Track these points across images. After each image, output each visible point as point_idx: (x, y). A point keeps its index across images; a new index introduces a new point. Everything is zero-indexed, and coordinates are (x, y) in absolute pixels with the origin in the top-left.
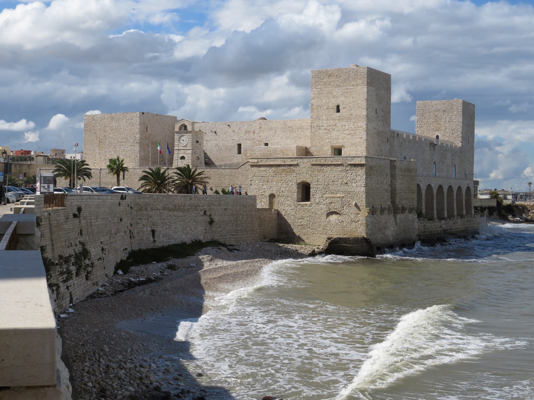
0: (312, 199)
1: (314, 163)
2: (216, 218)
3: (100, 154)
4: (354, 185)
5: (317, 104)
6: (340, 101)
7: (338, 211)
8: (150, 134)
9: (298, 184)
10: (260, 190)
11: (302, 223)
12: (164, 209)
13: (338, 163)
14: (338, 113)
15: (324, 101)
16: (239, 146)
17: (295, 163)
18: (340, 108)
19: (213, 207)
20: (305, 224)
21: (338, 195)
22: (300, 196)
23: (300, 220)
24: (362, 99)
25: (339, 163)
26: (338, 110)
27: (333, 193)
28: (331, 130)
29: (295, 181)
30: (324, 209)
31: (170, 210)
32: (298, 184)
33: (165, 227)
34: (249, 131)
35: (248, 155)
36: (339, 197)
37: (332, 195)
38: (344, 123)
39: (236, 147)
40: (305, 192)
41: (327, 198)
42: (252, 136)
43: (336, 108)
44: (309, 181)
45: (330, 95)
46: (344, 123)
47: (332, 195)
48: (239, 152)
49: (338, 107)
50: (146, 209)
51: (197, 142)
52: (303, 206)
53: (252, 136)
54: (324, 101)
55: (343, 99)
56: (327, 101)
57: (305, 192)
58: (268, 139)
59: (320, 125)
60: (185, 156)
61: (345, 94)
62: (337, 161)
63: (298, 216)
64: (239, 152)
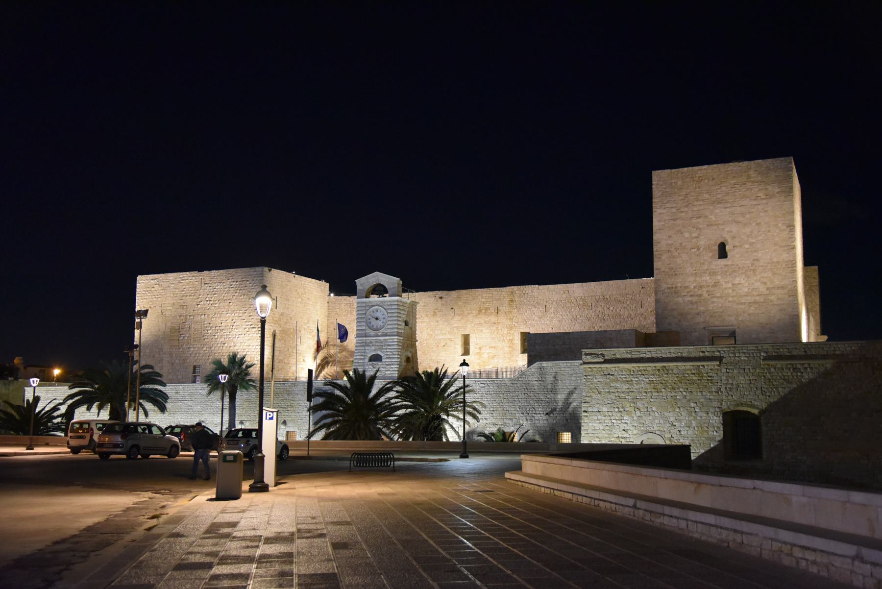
3: (171, 354)
5: (670, 242)
6: (728, 233)
8: (282, 314)
14: (723, 261)
15: (687, 235)
18: (727, 248)
24: (785, 227)
34: (486, 309)
35: (485, 356)
43: (717, 248)
45: (700, 220)
46: (737, 281)
54: (687, 235)
55: (734, 228)
56: (694, 235)
59: (679, 285)
60: (379, 353)
61: (741, 219)
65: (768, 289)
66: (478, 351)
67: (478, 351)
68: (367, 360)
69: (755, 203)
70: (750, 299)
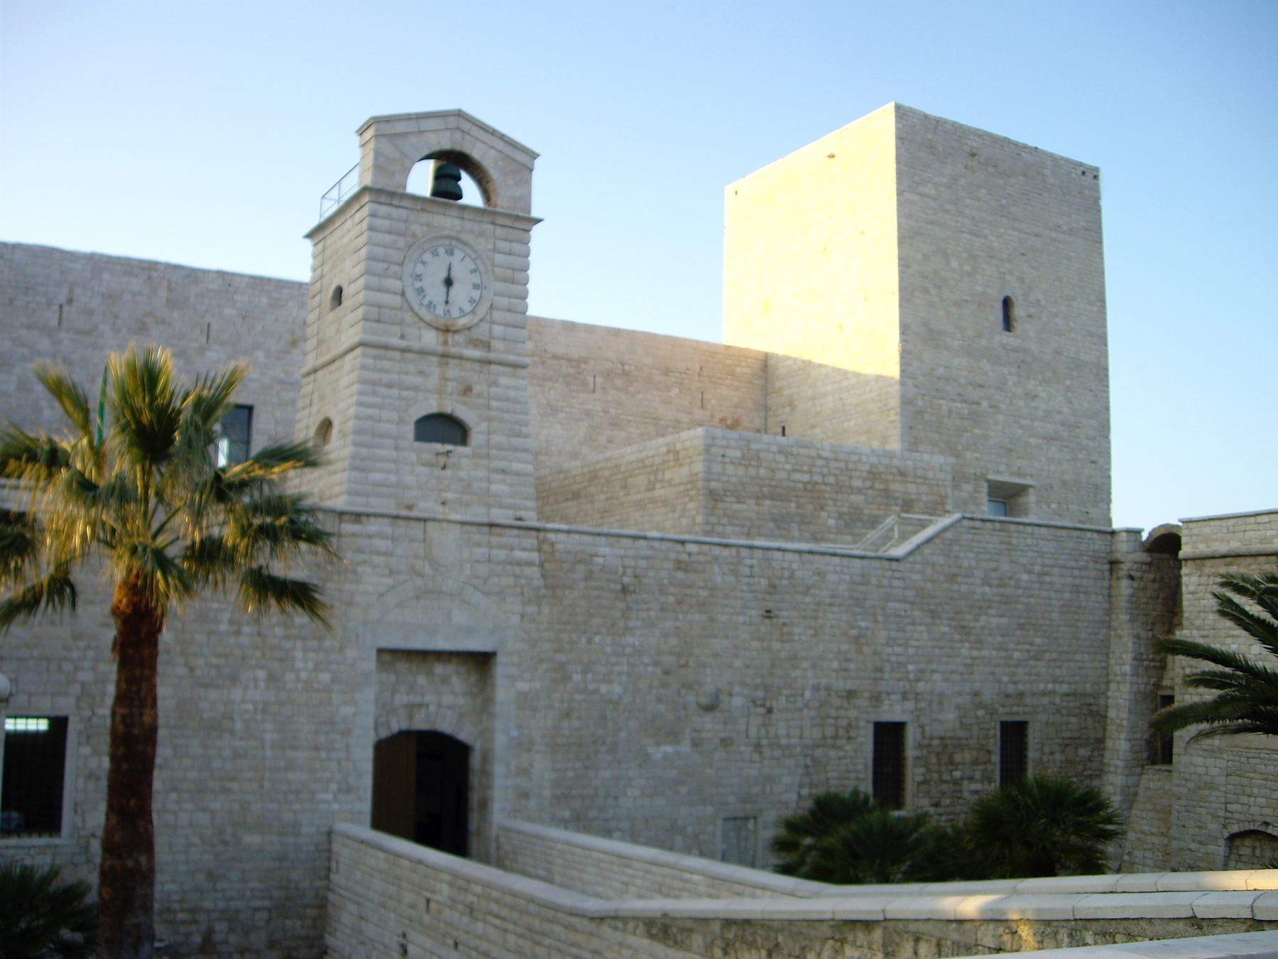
14: (1008, 338)
28: (985, 404)
38: (1031, 385)
56: (967, 268)
68: (410, 430)
70: (1050, 428)
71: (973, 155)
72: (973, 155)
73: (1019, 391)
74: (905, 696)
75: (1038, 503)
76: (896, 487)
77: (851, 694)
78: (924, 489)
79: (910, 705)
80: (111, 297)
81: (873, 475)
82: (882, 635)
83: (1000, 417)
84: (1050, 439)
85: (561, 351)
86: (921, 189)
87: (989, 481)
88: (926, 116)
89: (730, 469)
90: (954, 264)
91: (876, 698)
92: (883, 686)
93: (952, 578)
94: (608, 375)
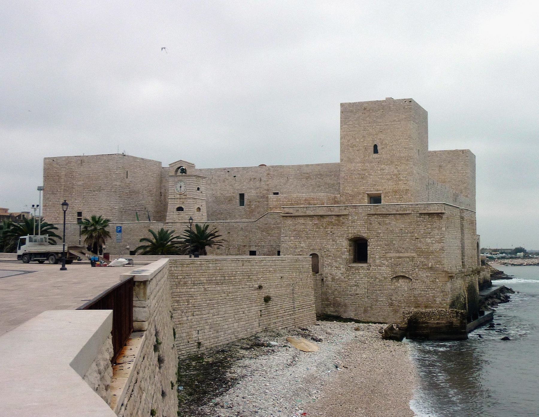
0: (370, 260)
1: (372, 212)
2: (272, 293)
4: (429, 241)
7: (407, 276)
9: (350, 240)
10: (296, 248)
11: (357, 292)
12: (210, 282)
13: (405, 212)
14: (376, 155)
16: (242, 196)
17: (347, 213)
19: (268, 275)
20: (361, 292)
21: (406, 255)
22: (352, 257)
23: (355, 288)
25: (408, 212)
26: (376, 151)
27: (398, 252)
28: (367, 174)
29: (345, 235)
30: (386, 271)
31: (217, 284)
32: (350, 240)
33: (212, 311)
34: (255, 179)
35: (253, 206)
36: (408, 257)
37: (398, 255)
38: (383, 166)
39: (238, 197)
40: (360, 250)
41: (391, 258)
42: (258, 184)
44: (365, 235)
46: (383, 166)
47: (398, 255)
48: (242, 203)
49: (375, 147)
50: (185, 283)
51: (198, 189)
52: (358, 269)
53: (258, 184)
56: (362, 140)
57: (360, 250)
58: (278, 187)
62: (404, 210)
63: (352, 282)
64: (242, 203)
65: (398, 171)
66: (249, 203)
67: (249, 203)
69: (393, 123)
70: (389, 177)
71: (365, 109)
72: (365, 109)
73: (379, 169)
74: (256, 246)
75: (385, 197)
76: (312, 202)
77: (245, 246)
78: (318, 201)
79: (257, 248)
80: (219, 176)
81: (306, 200)
82: (251, 236)
83: (371, 177)
84: (388, 180)
85: (305, 171)
86: (348, 123)
87: (368, 194)
88: (350, 103)
89: (274, 203)
90: (358, 140)
91: (250, 246)
92: (251, 244)
93: (266, 224)
94: (316, 175)
